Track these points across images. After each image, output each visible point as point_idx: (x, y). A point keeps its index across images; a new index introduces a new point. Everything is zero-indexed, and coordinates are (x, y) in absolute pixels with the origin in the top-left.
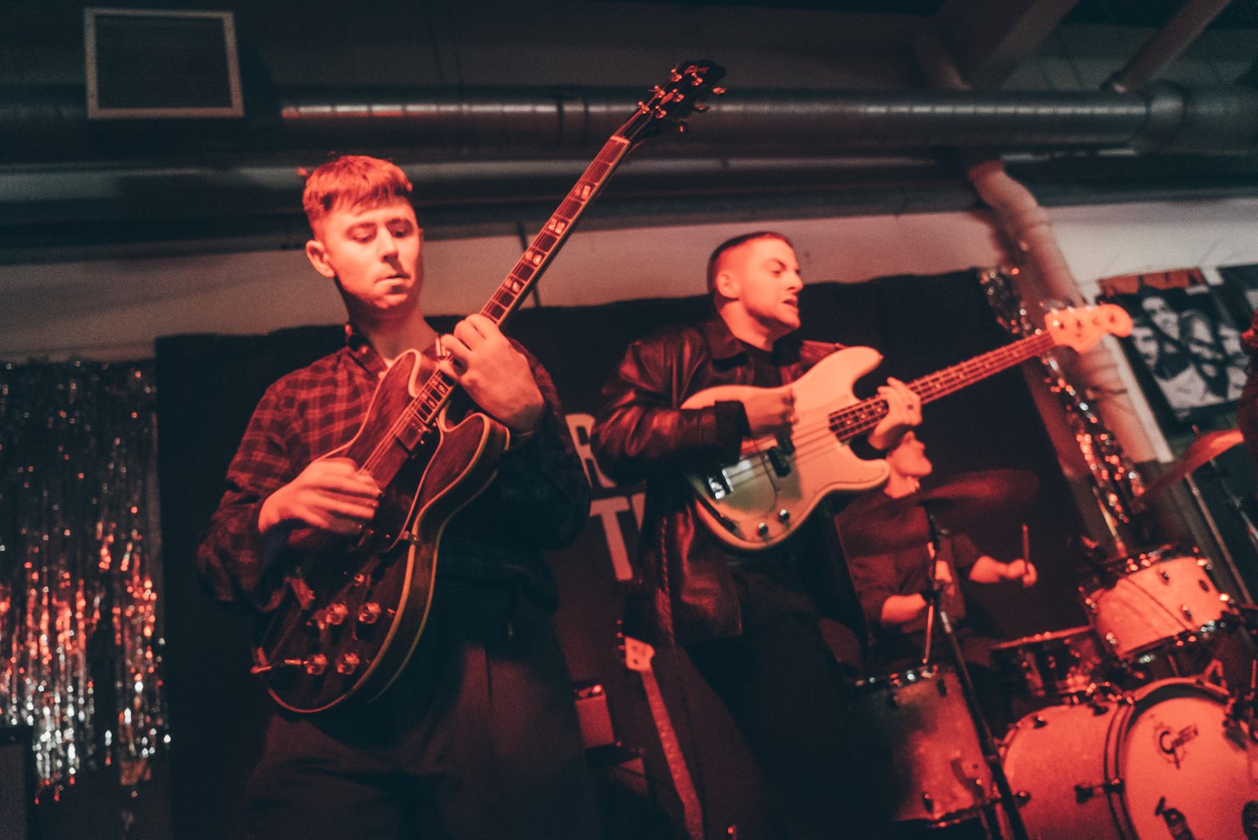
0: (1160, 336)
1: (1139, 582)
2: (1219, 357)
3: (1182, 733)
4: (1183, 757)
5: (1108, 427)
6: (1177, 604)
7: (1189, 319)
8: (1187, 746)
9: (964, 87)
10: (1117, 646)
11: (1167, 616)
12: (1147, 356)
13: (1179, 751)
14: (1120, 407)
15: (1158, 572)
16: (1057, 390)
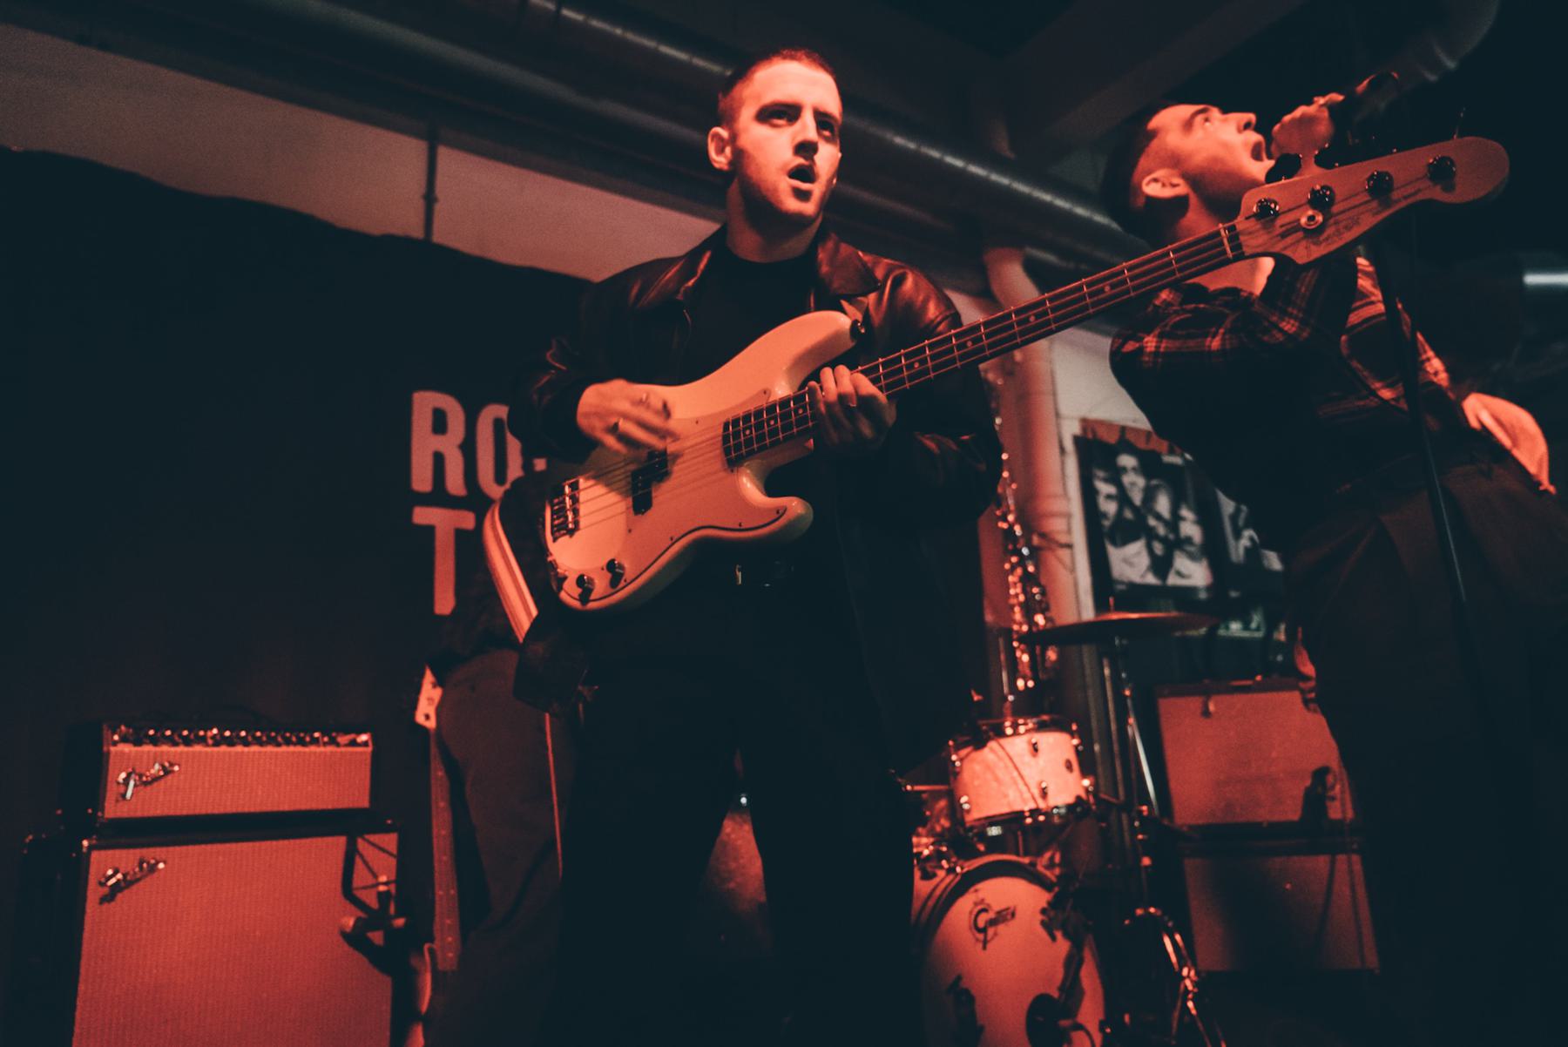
0: (1123, 498)
1: (1008, 748)
2: (1171, 536)
3: (999, 913)
4: (993, 938)
5: (1043, 582)
6: (1037, 779)
7: (1157, 487)
8: (1001, 928)
9: (1010, 154)
10: (968, 811)
11: (1024, 788)
12: (1105, 515)
13: (991, 932)
14: (1060, 561)
15: (1029, 742)
16: (1005, 526)
